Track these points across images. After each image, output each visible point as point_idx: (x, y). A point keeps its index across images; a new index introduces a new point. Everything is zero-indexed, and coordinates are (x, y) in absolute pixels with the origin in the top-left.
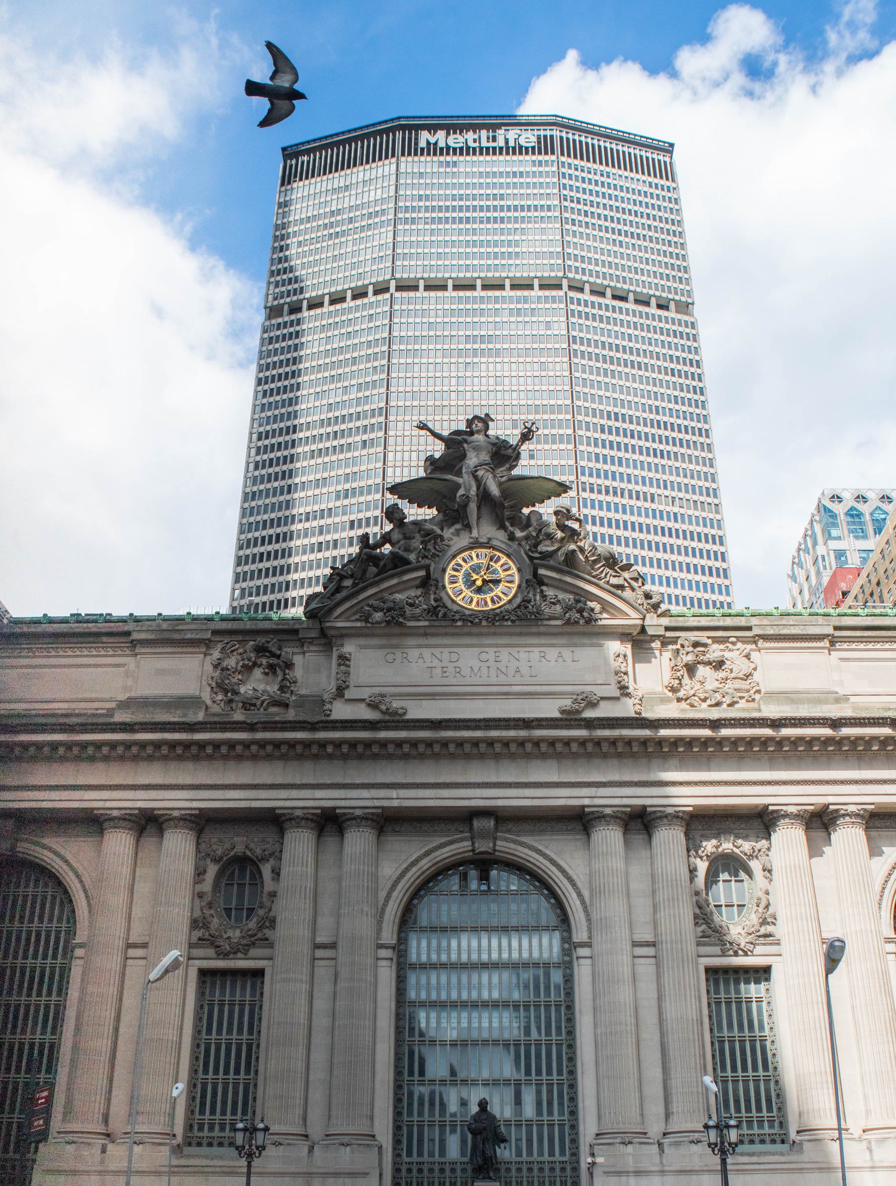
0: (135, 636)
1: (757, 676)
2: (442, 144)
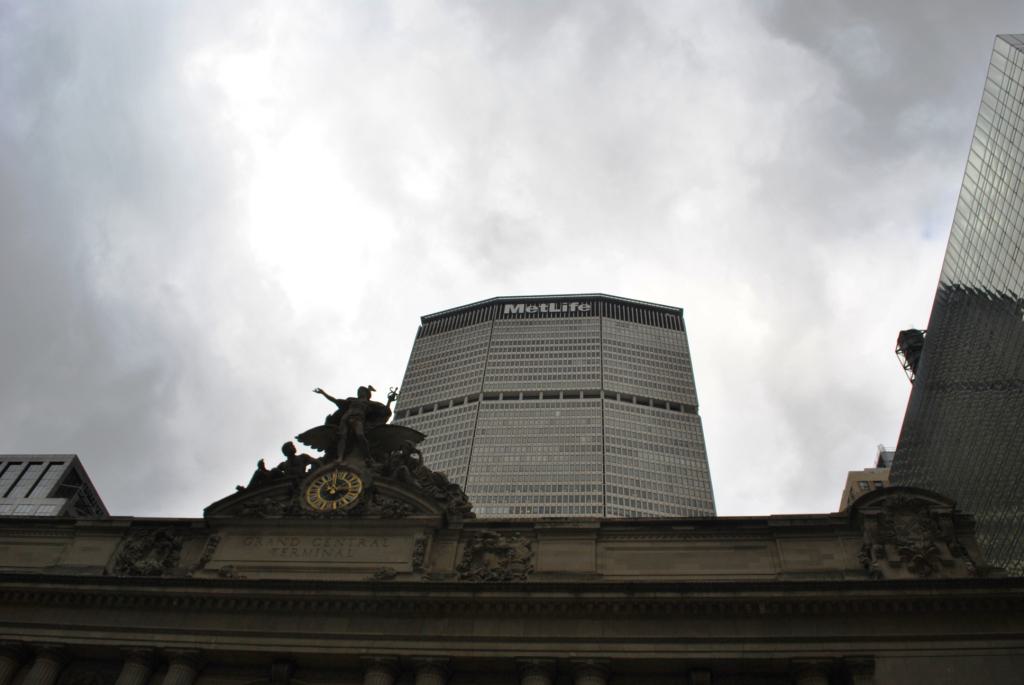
2: (521, 311)
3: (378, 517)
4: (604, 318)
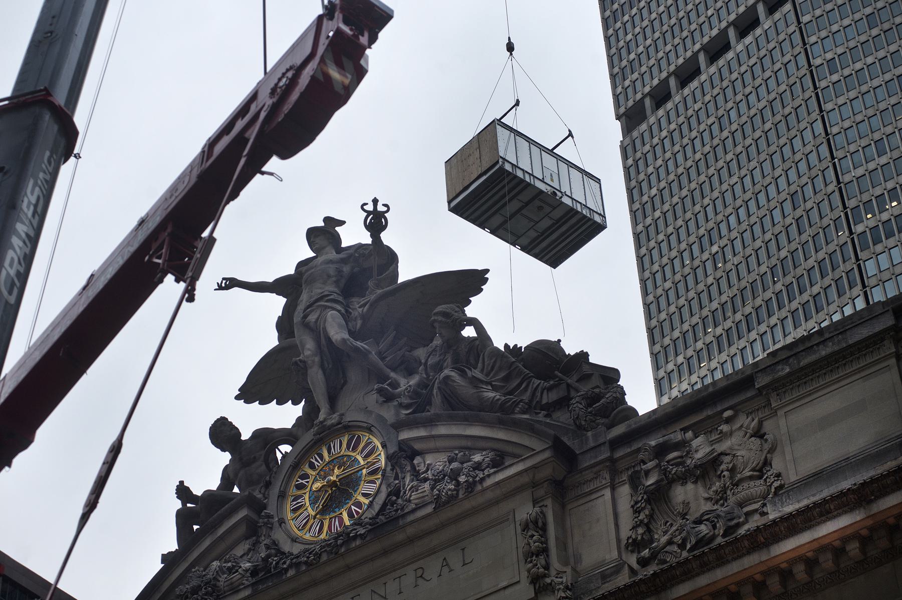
1: (777, 465)
3: (429, 509)
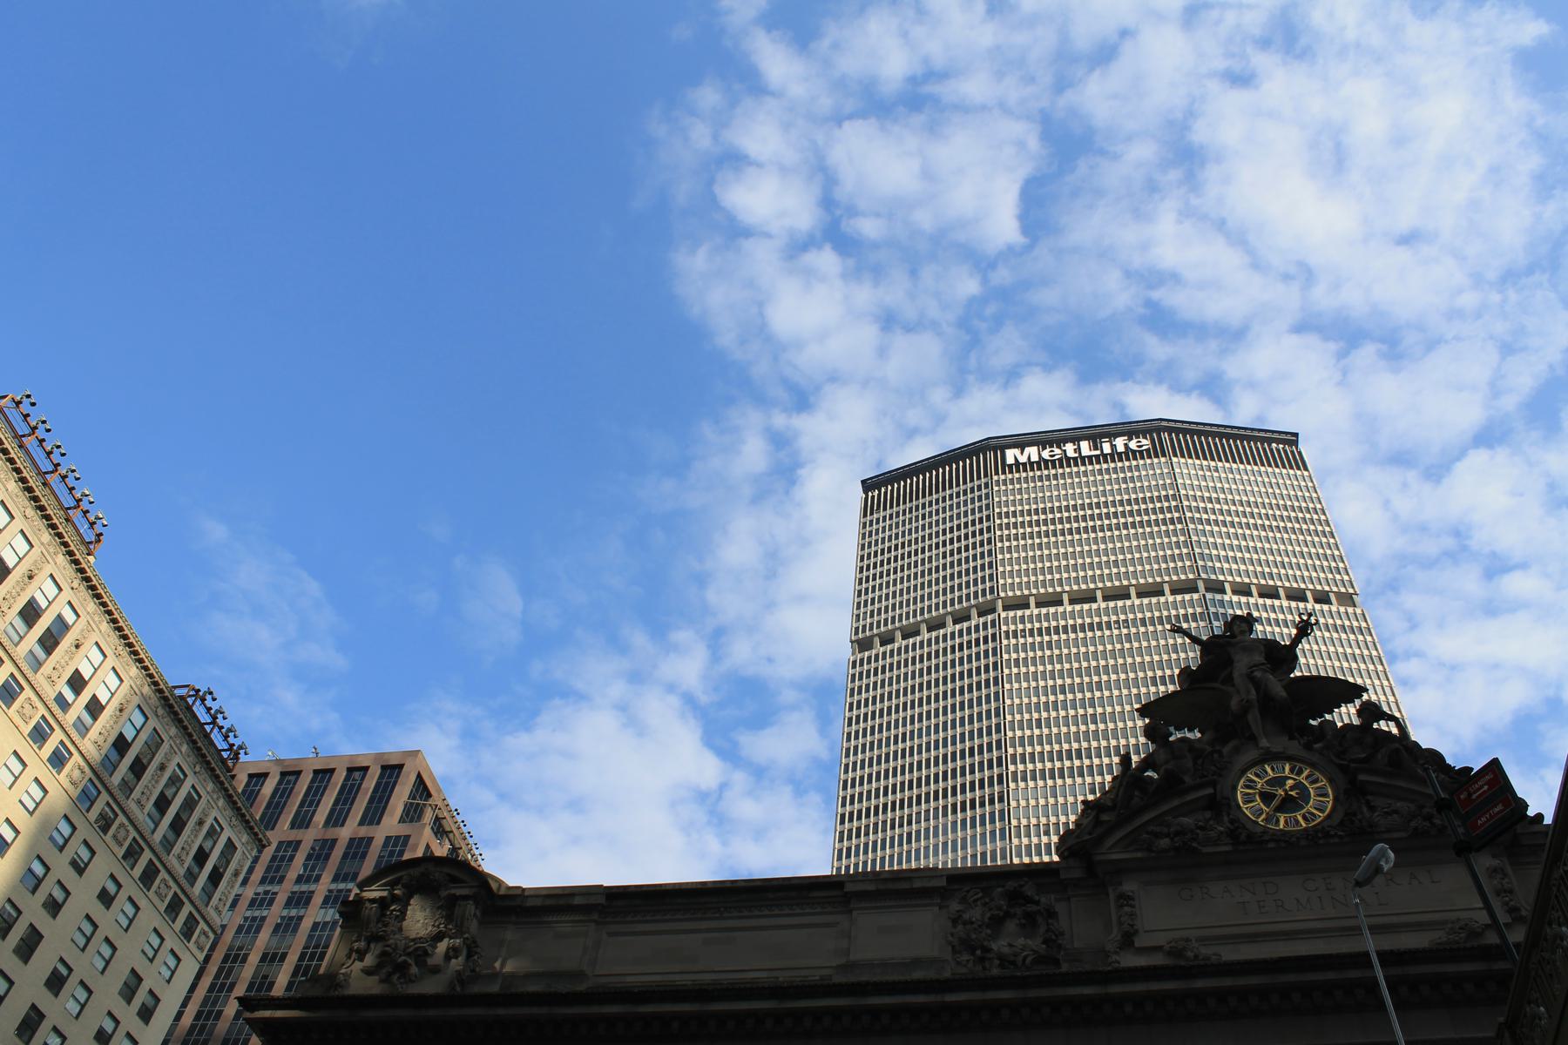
0: (849, 888)
2: (1035, 458)
3: (1403, 834)
4: (1175, 460)
